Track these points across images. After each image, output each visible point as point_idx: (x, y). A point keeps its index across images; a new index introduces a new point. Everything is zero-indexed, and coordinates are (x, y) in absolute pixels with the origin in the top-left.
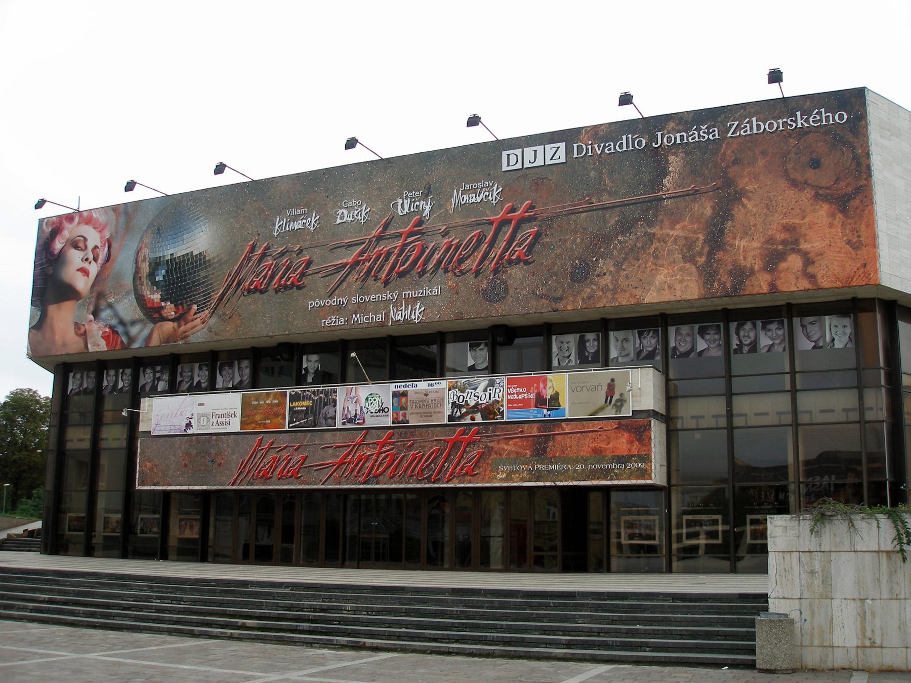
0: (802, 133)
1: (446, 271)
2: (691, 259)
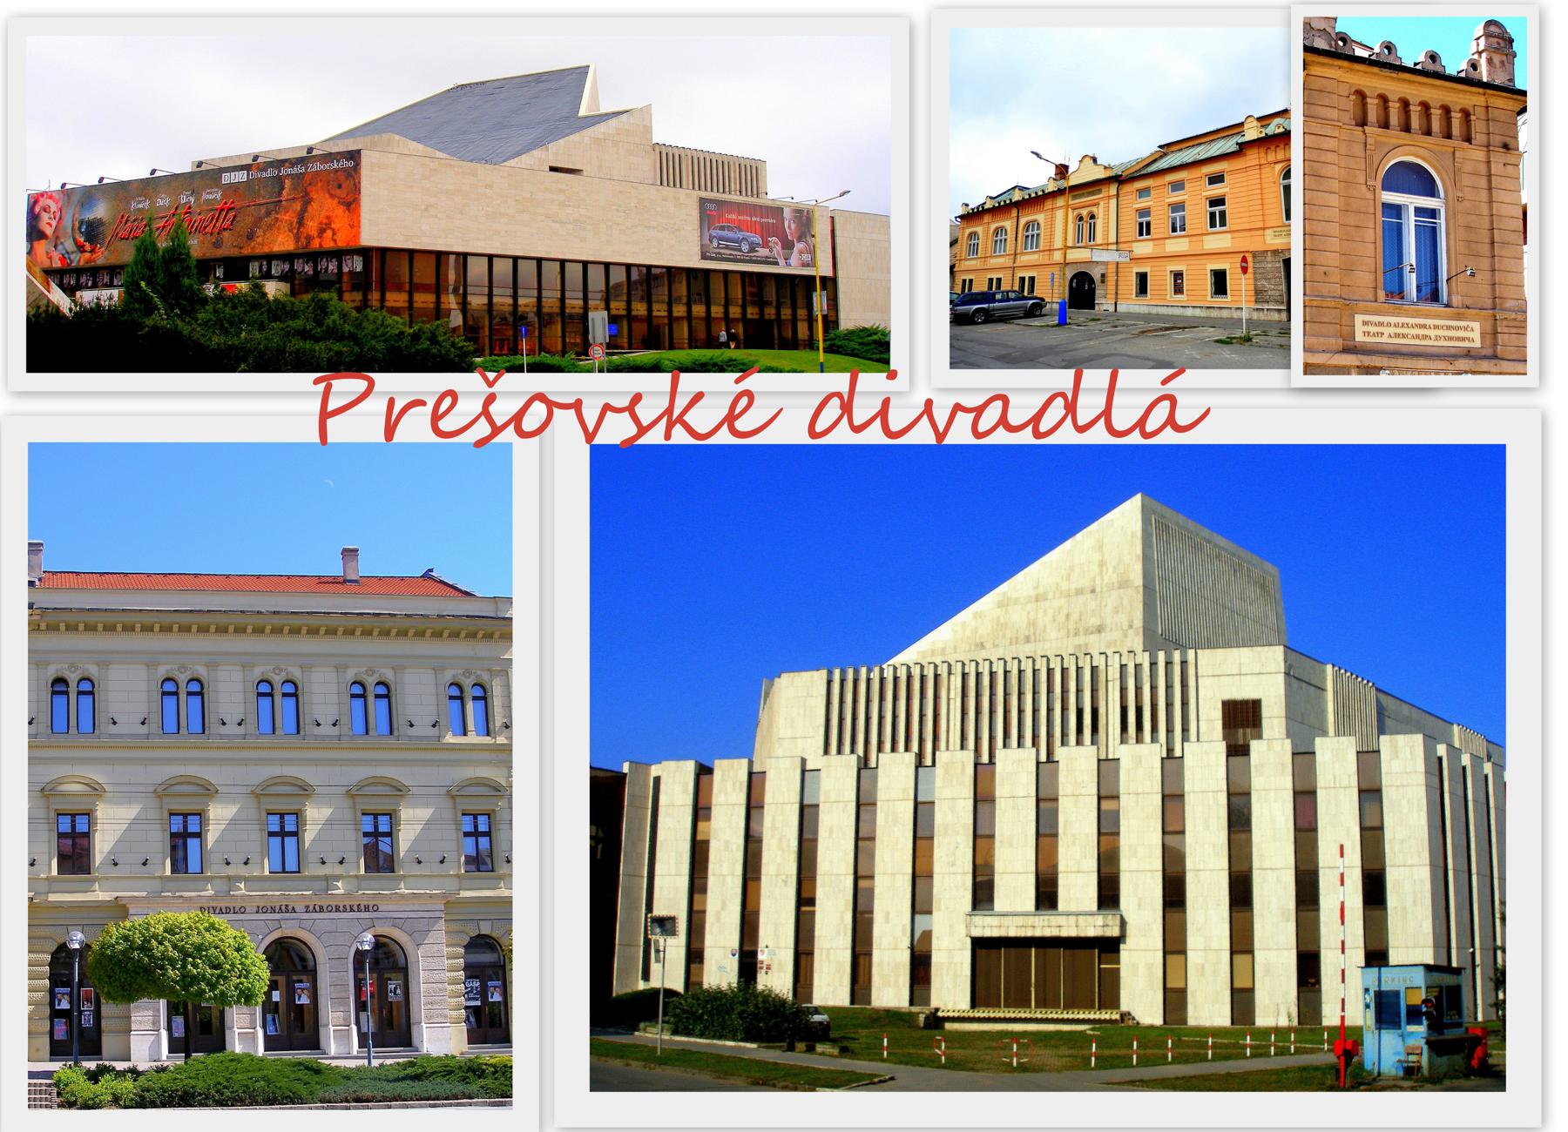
0: (336, 171)
2: (291, 230)
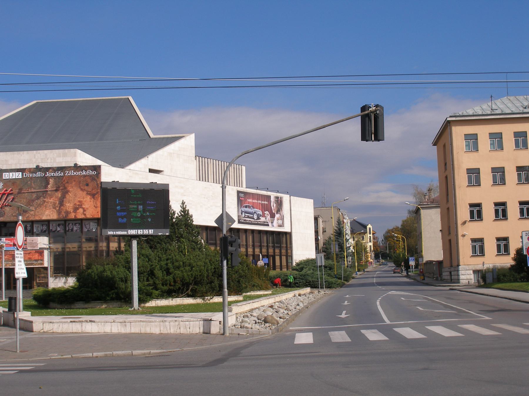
0: (85, 176)
2: (55, 208)
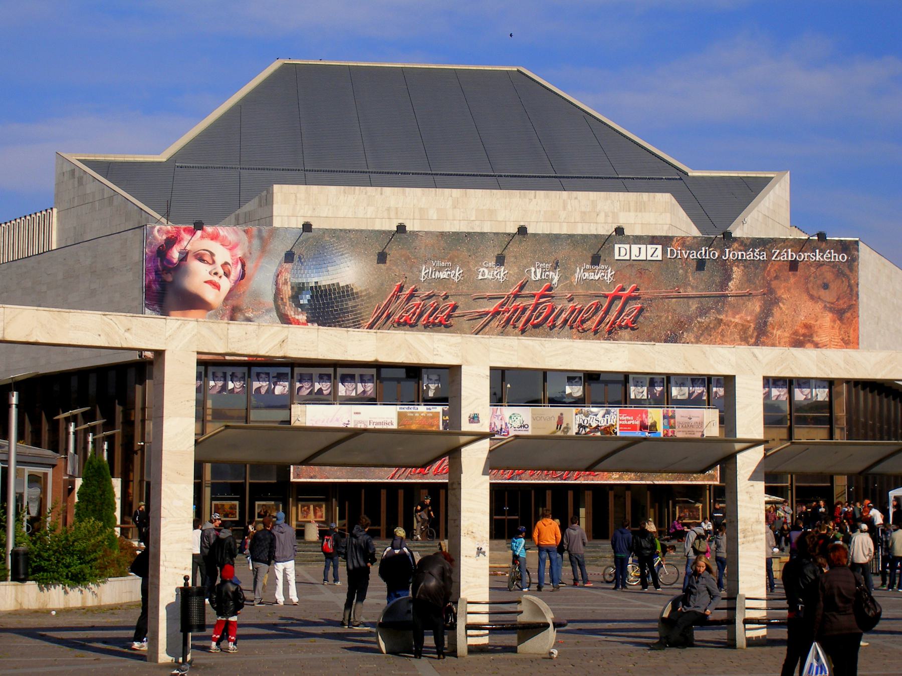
0: (819, 264)
1: (571, 328)
